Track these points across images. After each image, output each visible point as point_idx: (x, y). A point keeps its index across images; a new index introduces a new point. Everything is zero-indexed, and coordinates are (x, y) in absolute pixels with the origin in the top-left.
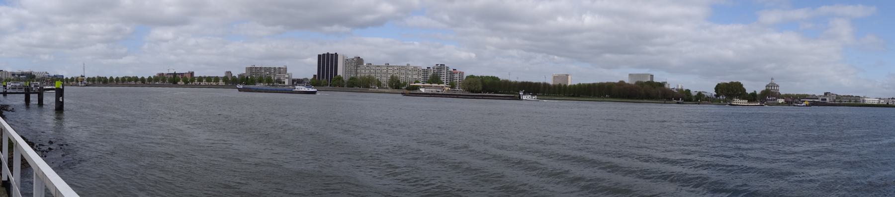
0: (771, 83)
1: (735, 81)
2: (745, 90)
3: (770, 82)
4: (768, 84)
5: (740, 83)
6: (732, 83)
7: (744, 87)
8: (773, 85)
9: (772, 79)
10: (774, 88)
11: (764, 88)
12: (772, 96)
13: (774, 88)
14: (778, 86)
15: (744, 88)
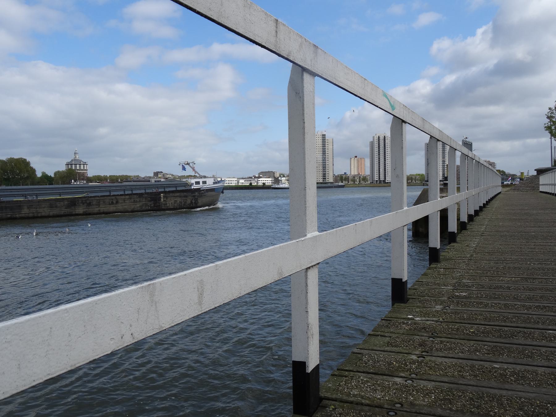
0: (75, 160)
1: (16, 157)
2: (34, 171)
3: (73, 157)
4: (69, 160)
5: (25, 160)
6: (11, 160)
7: (32, 165)
8: (79, 162)
9: (75, 154)
10: (80, 167)
11: (63, 168)
12: (80, 179)
13: (80, 167)
14: (85, 164)
15: (32, 168)
